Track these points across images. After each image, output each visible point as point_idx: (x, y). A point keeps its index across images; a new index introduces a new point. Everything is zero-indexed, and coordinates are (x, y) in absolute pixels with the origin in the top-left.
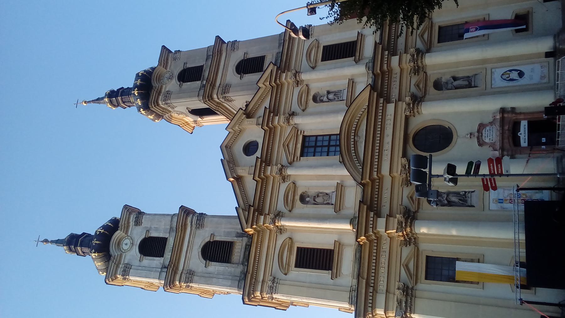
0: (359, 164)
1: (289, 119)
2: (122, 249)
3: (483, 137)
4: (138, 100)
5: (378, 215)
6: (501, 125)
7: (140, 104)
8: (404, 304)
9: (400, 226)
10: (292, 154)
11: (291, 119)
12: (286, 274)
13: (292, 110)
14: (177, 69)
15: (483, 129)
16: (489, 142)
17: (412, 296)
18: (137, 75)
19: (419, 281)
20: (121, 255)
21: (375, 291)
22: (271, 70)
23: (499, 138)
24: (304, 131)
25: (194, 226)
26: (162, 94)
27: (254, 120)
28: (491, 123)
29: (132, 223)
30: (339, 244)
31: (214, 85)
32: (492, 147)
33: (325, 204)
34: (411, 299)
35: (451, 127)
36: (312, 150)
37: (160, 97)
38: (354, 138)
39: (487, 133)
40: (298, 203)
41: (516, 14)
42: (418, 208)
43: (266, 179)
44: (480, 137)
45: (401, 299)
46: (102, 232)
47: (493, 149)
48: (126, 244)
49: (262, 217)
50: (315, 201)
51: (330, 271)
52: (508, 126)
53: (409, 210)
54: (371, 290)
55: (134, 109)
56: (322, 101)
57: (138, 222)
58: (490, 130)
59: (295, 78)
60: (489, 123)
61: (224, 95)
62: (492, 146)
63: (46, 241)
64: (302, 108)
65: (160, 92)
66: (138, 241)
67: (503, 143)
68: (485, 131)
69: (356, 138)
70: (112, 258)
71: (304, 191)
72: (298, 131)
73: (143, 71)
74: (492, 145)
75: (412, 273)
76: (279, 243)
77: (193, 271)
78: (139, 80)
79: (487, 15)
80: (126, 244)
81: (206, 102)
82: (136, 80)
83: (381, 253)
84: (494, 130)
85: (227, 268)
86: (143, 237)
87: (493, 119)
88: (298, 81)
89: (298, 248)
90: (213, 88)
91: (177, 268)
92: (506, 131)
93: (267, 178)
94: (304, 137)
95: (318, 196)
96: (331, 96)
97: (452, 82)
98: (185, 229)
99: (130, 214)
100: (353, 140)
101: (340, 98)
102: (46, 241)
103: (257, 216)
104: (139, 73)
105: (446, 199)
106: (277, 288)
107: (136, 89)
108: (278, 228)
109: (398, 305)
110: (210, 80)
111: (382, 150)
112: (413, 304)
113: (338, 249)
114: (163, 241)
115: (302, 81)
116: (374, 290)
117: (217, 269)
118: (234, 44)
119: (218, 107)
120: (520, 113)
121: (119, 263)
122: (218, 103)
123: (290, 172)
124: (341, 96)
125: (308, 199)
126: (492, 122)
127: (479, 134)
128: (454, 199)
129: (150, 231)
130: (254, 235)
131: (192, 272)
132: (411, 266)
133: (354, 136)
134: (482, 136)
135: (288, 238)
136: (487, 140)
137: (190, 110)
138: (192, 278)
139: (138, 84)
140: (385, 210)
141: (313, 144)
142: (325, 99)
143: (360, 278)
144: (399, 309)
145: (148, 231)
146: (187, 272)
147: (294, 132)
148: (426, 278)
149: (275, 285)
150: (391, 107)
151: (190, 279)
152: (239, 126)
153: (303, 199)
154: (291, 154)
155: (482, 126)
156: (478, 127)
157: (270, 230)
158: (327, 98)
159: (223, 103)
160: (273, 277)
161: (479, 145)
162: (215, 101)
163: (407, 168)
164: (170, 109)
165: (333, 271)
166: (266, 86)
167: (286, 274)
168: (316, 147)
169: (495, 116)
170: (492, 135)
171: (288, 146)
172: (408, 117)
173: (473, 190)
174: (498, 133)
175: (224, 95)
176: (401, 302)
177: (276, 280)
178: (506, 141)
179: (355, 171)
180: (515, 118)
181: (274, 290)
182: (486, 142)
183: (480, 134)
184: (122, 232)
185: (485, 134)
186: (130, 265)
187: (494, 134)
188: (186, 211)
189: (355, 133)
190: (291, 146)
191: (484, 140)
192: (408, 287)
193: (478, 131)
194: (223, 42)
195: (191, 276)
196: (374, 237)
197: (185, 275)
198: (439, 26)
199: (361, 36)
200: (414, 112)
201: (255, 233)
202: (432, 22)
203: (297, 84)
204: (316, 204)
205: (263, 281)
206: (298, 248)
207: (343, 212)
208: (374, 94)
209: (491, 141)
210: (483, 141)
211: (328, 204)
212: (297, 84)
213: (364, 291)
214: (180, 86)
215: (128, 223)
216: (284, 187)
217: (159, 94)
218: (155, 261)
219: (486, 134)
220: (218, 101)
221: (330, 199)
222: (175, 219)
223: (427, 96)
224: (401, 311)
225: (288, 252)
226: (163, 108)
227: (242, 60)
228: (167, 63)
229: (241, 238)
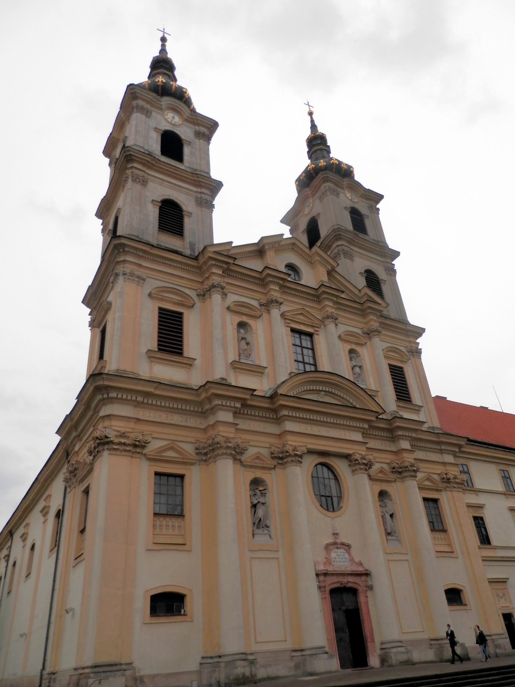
0: (295, 393)
1: (332, 318)
2: (167, 111)
3: (336, 550)
4: (325, 164)
5: (236, 413)
8: (123, 441)
9: (226, 440)
10: (293, 318)
11: (332, 320)
12: (150, 295)
13: (339, 324)
14: (363, 208)
15: (345, 550)
17: (133, 453)
18: (351, 167)
19: (152, 463)
20: (161, 109)
21: (137, 404)
22: (380, 304)
23: (337, 569)
24: (318, 335)
25: (199, 196)
26: (336, 187)
27: (325, 278)
28: (352, 560)
29: (197, 128)
30: (189, 364)
32: (327, 561)
33: (239, 351)
34: (129, 451)
35: (342, 510)
36: (298, 343)
37: (333, 185)
38: (323, 391)
39: (342, 554)
40: (238, 319)
41: (461, 590)
42: (245, 466)
43: (263, 284)
44: (336, 546)
45: (129, 437)
46: (185, 95)
48: (173, 118)
49: (220, 272)
50: (241, 340)
51: (157, 350)
53: (241, 453)
54: (140, 399)
56: (351, 359)
57: (198, 135)
58: (345, 558)
59: (375, 330)
61: (341, 253)
62: (328, 561)
63: (163, 40)
64: (342, 335)
65: (337, 186)
66: (177, 131)
67: (333, 574)
68: (343, 552)
69: (323, 393)
70: (159, 97)
71: (254, 327)
72: (318, 328)
74: (328, 561)
75: (163, 455)
76: (187, 291)
77: (147, 185)
78: (346, 167)
79: (458, 555)
80: (173, 118)
81: (333, 231)
82: (346, 165)
83: (184, 417)
85: (152, 225)
86: (183, 137)
88: (369, 334)
89: (181, 314)
90: (348, 242)
91: (149, 168)
93: (263, 285)
94: (310, 335)
95: (248, 344)
96: (357, 369)
97: (388, 513)
98: (196, 186)
99: (208, 129)
100: (321, 389)
101: (357, 381)
102: (163, 40)
103: (222, 267)
104: (353, 169)
105: (259, 502)
106: (132, 282)
107: (337, 163)
108: (207, 291)
109: (122, 433)
111: (312, 424)
112: (123, 453)
113: (185, 362)
114: (179, 158)
115: (370, 339)
116: (139, 403)
117: (150, 213)
118: (392, 272)
119: (325, 247)
120: (367, 597)
121: (152, 105)
122: (330, 247)
123: (276, 313)
124: (358, 382)
125: (242, 331)
126: (354, 561)
127: (340, 544)
128: (260, 512)
129: (189, 147)
130: (196, 261)
131: (146, 184)
132: (171, 454)
133: (325, 391)
134: (337, 548)
135: (194, 303)
136: (333, 555)
137: (316, 218)
138: (139, 183)
140: (244, 424)
141: (304, 345)
142: (354, 363)
143: (156, 385)
144: (116, 433)
145: (189, 143)
146: (146, 179)
147: (317, 322)
148: (157, 474)
149: (136, 279)
150: (357, 437)
151: (138, 180)
152: (319, 261)
153: (242, 325)
154: (291, 316)
155: (347, 547)
157: (202, 283)
158: (355, 365)
159: (331, 252)
160: (146, 278)
162: (333, 243)
163: (296, 452)
164: (317, 195)
165: (159, 353)
166: (362, 297)
167: (150, 295)
168: (302, 347)
169: (361, 564)
170: (340, 561)
171: (301, 314)
172: (349, 457)
173: (272, 536)
174: (343, 569)
175: (341, 253)
176: (125, 437)
177: (142, 282)
178: (335, 579)
179: (289, 388)
181: (130, 277)
184: (188, 115)
185: (340, 552)
186: (150, 116)
188: (216, 186)
189: (328, 392)
190: (301, 317)
191: (333, 552)
192: (144, 447)
193: (343, 544)
194: (393, 259)
195: (142, 181)
196: (207, 407)
197: (142, 175)
198: (439, 499)
199: (417, 409)
200: (355, 464)
201: (198, 263)
202: (441, 491)
203: (366, 333)
204: (238, 341)
205: (140, 265)
206: (181, 314)
207: (232, 372)
208: (373, 416)
209: (333, 560)
210: (333, 549)
211: (240, 355)
212: (366, 333)
213: (139, 388)
214: (345, 208)
215: (198, 125)
216: (255, 303)
217: (335, 184)
218: (155, 145)
219: (340, 554)
220: (334, 246)
221: (246, 357)
222: (205, 175)
223: (371, 482)
224: (114, 437)
225: (178, 300)
226: (319, 187)
228: (367, 199)
229: (189, 248)
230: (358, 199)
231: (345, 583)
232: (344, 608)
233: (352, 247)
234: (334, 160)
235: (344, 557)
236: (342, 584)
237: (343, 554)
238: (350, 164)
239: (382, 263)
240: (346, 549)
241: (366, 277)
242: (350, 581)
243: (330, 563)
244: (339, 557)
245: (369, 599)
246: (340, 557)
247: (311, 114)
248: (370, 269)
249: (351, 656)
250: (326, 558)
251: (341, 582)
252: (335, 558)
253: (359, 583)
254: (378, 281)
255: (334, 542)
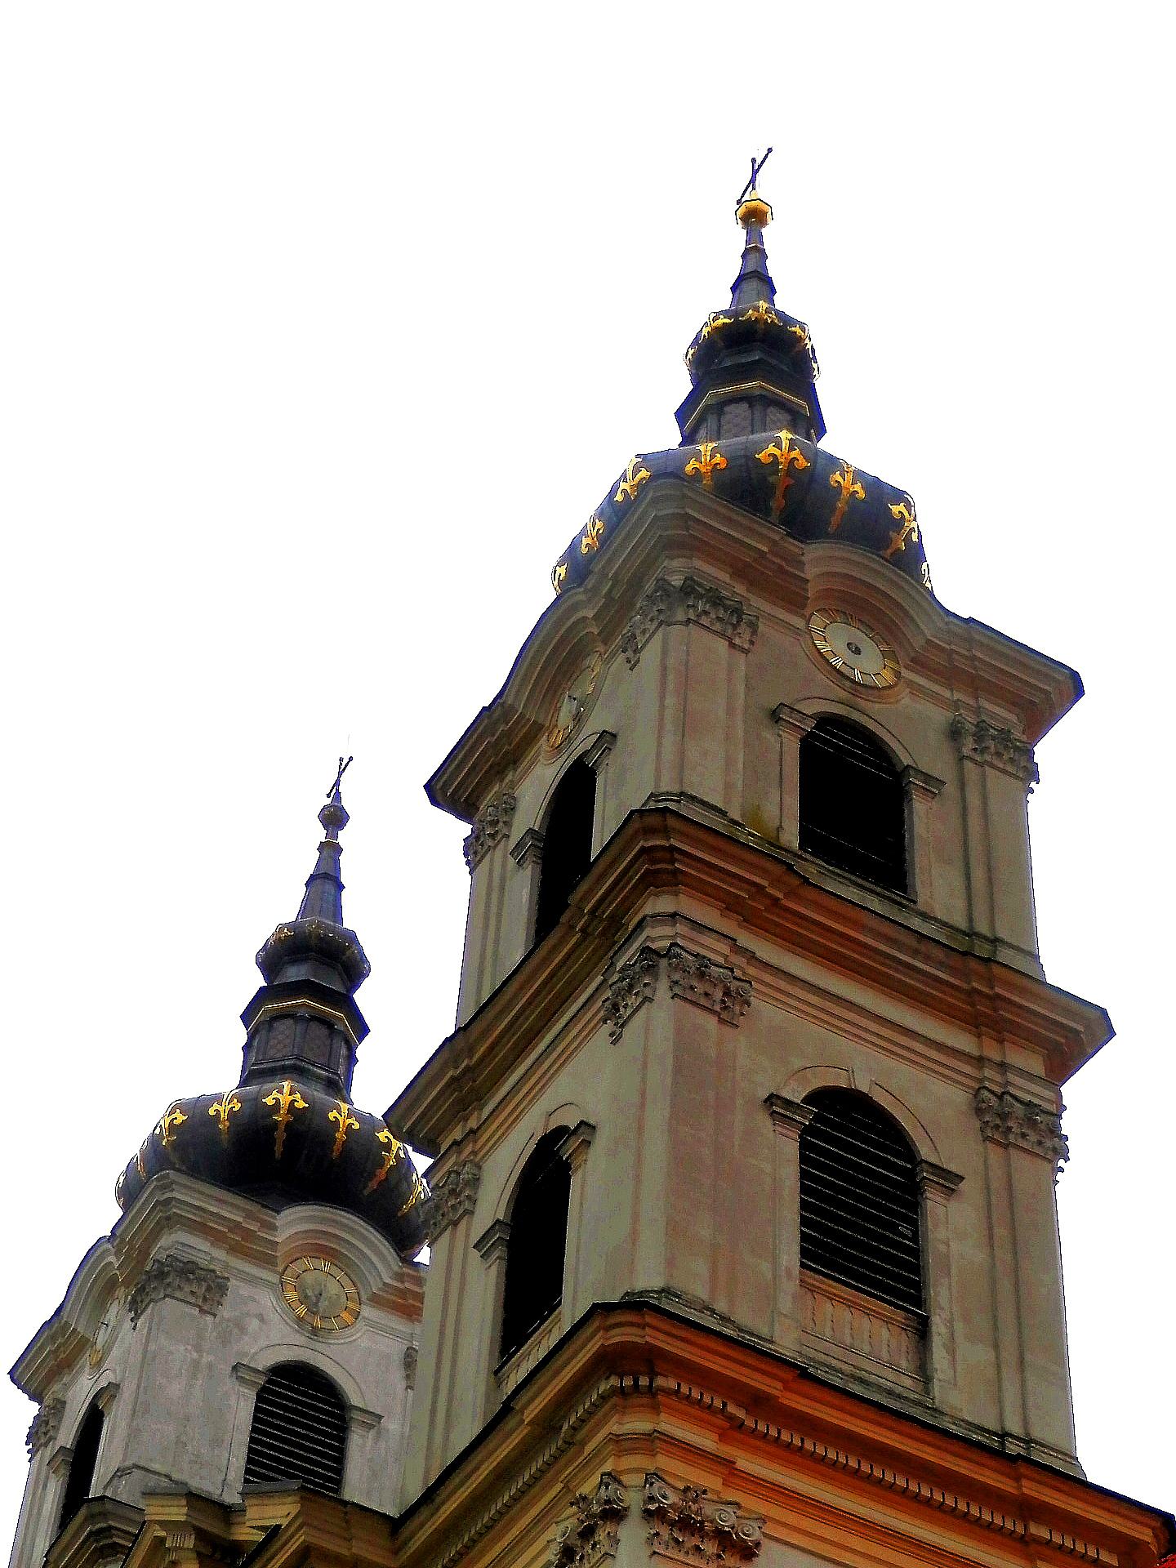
7: (689, 468)
31: (752, 921)
55: (669, 437)
73: (915, 537)
78: (858, 487)
82: (859, 475)
90: (731, 906)
104: (909, 506)
110: (791, 894)
139: (837, 477)
217: (740, 571)
227: (907, 1149)
230: (898, 674)
233: (745, 939)
234: (778, 446)
238: (892, 477)
239: (967, 1069)
241: (806, 1131)
247: (754, 218)
248: (864, 1088)
254: (910, 1175)
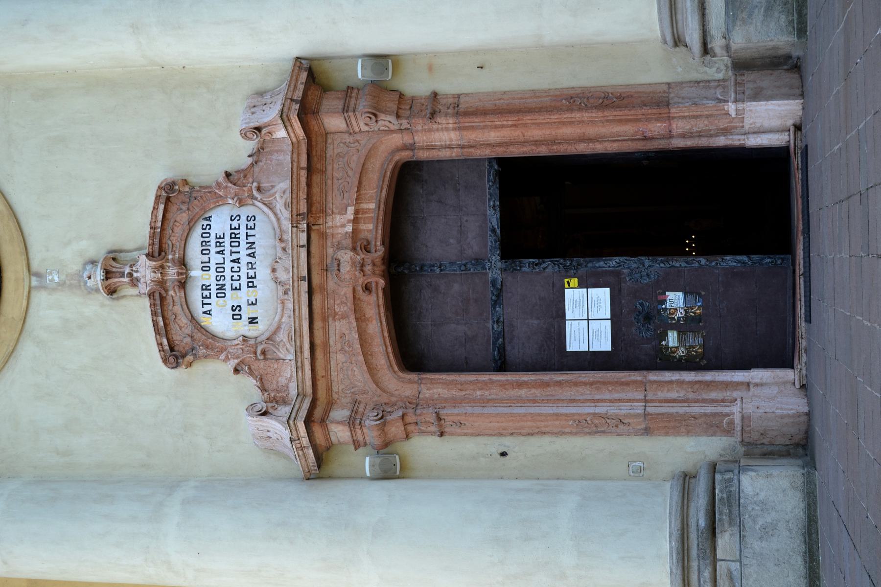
3: (196, 295)
6: (303, 208)
16: (230, 334)
32: (251, 373)
39: (215, 259)
44: (173, 293)
47: (263, 389)
52: (351, 210)
58: (234, 237)
60: (228, 175)
68: (205, 251)
84: (264, 239)
87: (251, 145)
92: (339, 247)
126: (245, 173)
134: (183, 285)
156: (155, 208)
161: (165, 361)
169: (258, 129)
180: (397, 140)
182: (214, 336)
183: (172, 272)
185: (205, 268)
187: (263, 273)
191: (205, 321)
209: (242, 328)
210: (193, 319)
231: (362, 266)
232: (495, 267)
235: (227, 240)
236: (367, 288)
237: (213, 249)
240: (183, 217)
242: (349, 228)
243: (264, 353)
244: (228, 282)
245: (447, 86)
246: (228, 274)
249: (730, 261)
250: (236, 371)
251: (359, 288)
252: (236, 311)
253: (364, 152)
255: (153, 305)
